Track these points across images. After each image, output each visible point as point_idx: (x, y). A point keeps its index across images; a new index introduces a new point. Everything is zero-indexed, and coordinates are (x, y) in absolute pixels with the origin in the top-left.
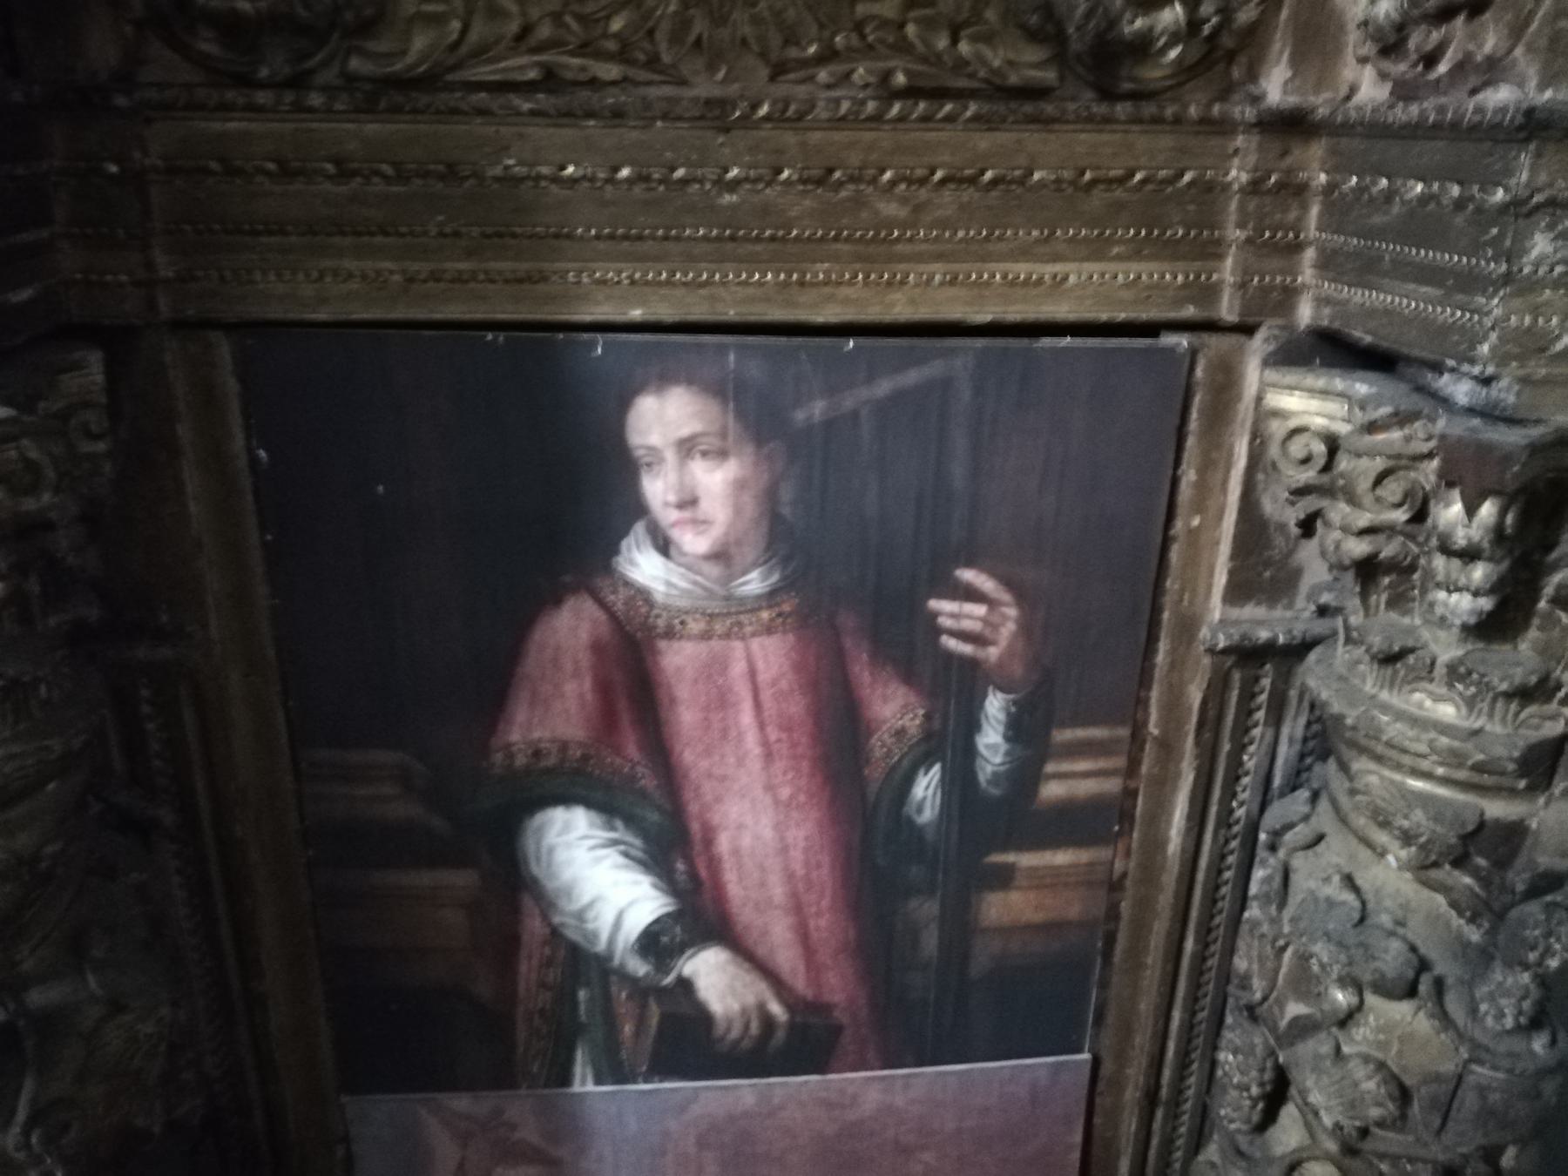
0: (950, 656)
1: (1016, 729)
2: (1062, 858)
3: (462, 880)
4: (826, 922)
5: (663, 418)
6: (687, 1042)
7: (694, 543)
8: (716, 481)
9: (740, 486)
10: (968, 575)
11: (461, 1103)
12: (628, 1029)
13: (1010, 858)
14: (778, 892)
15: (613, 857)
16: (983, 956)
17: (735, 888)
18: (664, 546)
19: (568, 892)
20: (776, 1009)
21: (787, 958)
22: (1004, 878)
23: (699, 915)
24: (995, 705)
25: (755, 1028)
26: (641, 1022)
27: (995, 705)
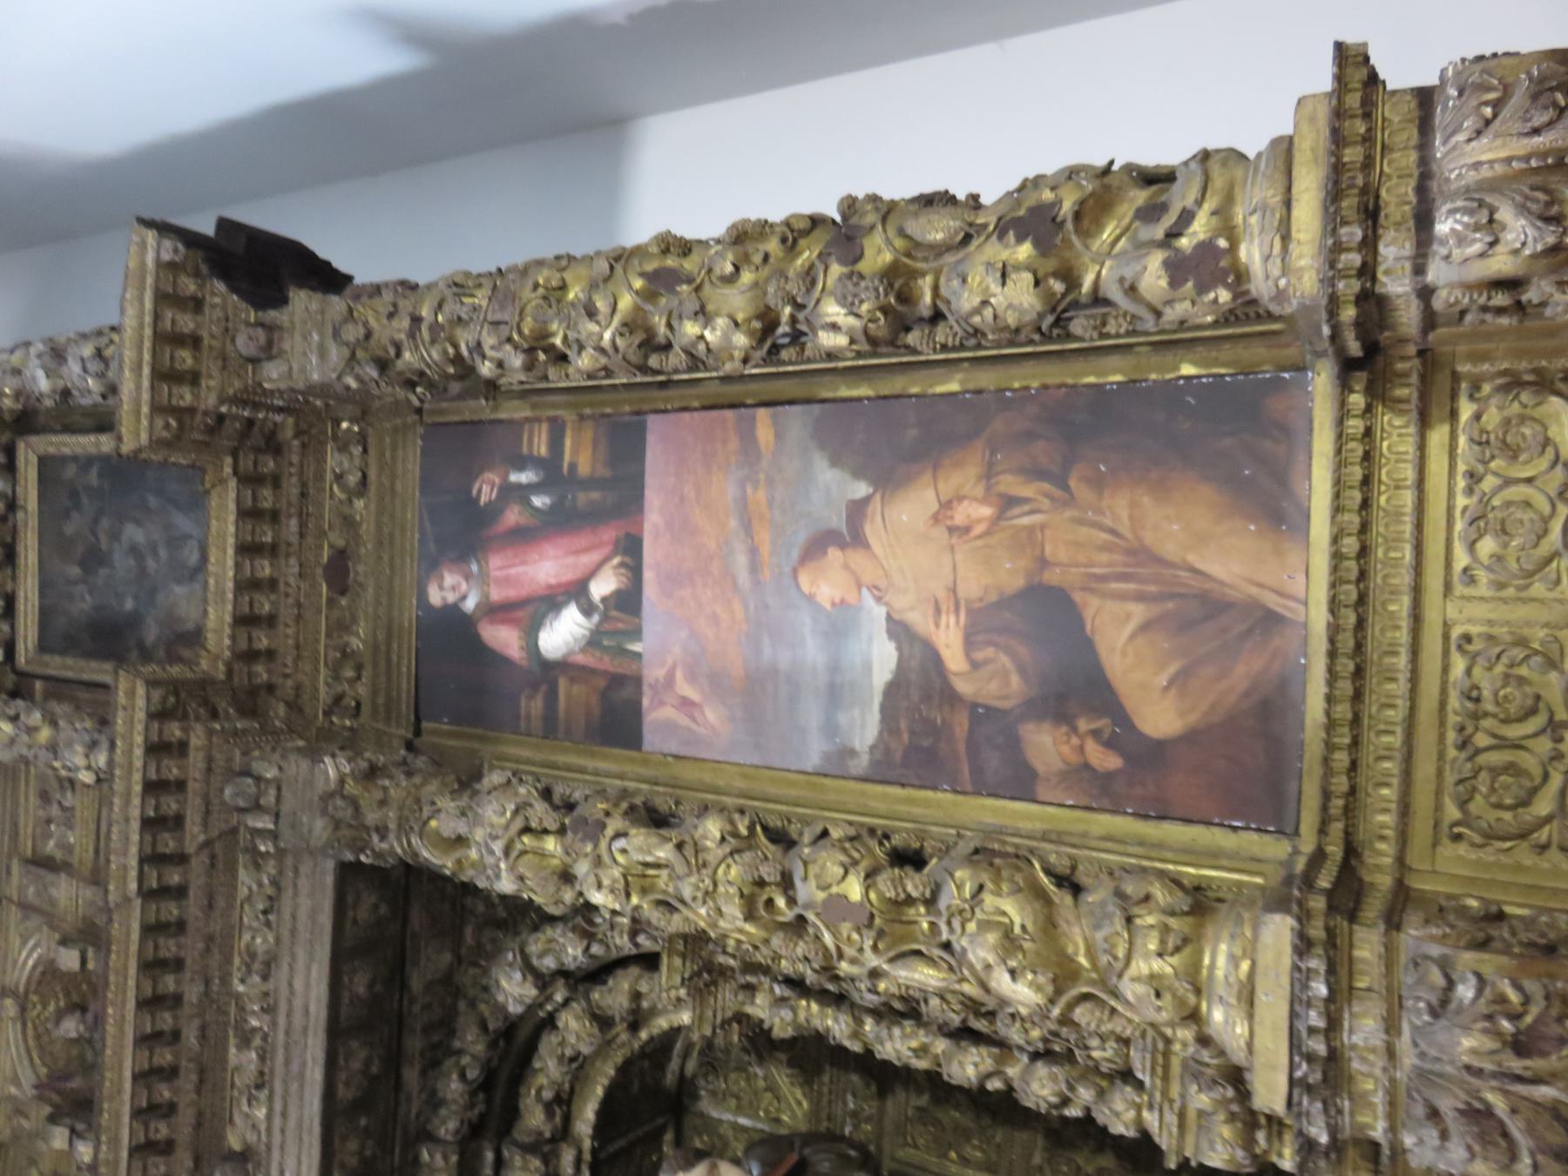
0: (498, 496)
1: (521, 468)
2: (568, 443)
3: (562, 684)
4: (582, 541)
5: (435, 597)
6: (628, 601)
7: (464, 586)
8: (450, 579)
9: (450, 571)
10: (474, 492)
11: (646, 702)
12: (620, 626)
13: (565, 465)
14: (571, 560)
15: (556, 624)
16: (603, 472)
17: (569, 576)
18: (464, 598)
19: (567, 643)
20: (616, 561)
21: (595, 557)
22: (573, 466)
23: (577, 591)
24: (515, 477)
25: (623, 571)
26: (618, 620)
27: (515, 477)
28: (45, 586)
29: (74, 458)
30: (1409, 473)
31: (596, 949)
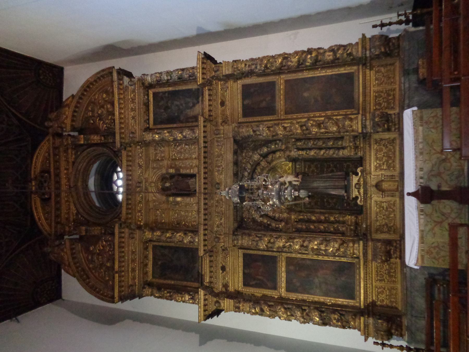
28: (154, 115)
29: (162, 92)
30: (369, 75)
31: (269, 149)
